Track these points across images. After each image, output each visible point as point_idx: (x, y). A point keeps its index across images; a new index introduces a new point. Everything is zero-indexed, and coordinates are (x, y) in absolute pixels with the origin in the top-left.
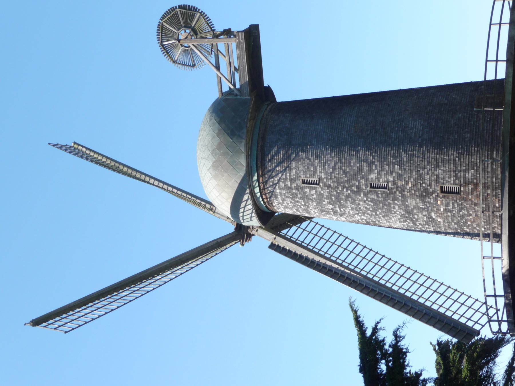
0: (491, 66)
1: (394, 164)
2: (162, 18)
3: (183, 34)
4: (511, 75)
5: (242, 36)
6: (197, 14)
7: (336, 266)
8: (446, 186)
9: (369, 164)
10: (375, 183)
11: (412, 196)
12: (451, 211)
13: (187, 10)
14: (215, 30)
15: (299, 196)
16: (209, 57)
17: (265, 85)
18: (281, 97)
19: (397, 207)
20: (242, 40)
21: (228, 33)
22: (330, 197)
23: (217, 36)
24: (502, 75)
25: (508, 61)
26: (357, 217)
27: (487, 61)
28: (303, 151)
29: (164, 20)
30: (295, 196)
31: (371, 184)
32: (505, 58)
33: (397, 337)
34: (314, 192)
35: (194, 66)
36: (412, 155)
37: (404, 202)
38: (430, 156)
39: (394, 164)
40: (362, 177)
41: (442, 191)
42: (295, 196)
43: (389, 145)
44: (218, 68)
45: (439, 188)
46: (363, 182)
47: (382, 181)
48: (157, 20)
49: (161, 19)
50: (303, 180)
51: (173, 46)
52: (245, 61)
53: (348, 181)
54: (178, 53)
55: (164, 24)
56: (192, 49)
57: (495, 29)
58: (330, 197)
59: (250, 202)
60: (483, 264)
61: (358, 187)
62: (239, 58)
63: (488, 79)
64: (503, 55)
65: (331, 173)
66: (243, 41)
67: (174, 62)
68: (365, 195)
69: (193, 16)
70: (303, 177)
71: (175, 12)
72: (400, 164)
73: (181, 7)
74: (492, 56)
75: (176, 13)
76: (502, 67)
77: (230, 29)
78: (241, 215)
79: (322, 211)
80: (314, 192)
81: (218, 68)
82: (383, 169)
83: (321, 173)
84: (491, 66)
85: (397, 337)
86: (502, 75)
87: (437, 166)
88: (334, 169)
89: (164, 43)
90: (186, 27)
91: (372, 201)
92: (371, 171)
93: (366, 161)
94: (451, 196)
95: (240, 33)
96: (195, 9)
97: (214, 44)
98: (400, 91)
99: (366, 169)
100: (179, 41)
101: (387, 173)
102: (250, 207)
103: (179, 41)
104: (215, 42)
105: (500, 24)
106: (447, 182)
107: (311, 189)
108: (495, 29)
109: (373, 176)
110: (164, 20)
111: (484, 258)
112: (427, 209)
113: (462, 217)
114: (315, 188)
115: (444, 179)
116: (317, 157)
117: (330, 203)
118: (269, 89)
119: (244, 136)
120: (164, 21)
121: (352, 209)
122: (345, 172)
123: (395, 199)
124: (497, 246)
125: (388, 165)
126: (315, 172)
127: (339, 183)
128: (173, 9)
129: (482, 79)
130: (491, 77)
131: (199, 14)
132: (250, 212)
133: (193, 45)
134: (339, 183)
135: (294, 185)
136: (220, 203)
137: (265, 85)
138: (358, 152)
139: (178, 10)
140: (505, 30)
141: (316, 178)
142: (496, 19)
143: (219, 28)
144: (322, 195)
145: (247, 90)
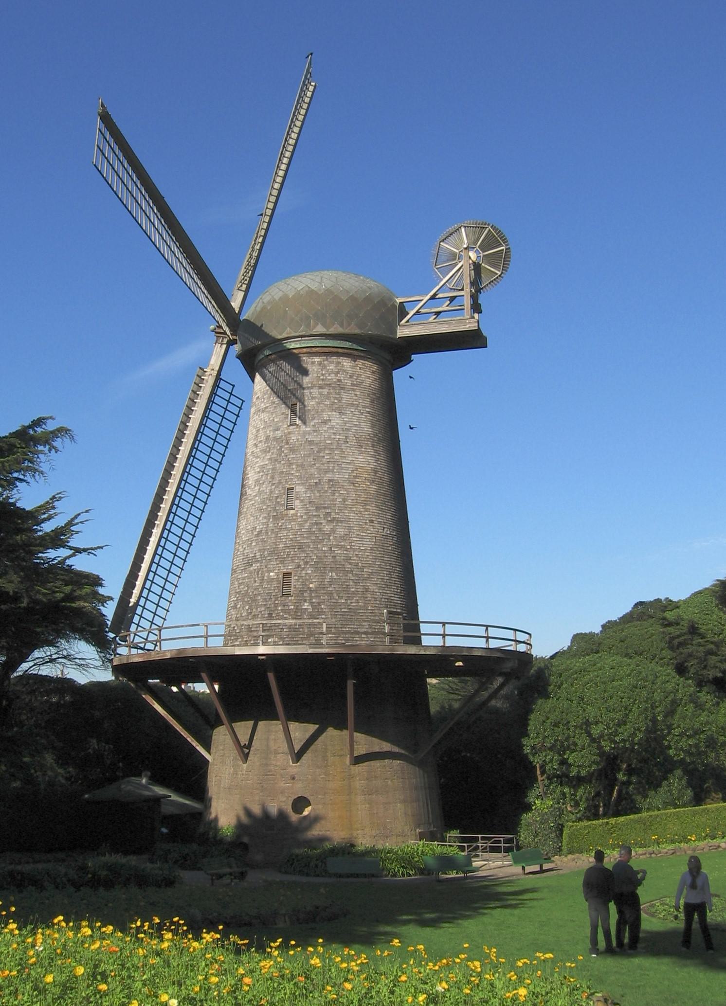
0: (439, 629)
6: (499, 271)
13: (504, 258)
14: (481, 293)
17: (413, 357)
18: (399, 376)
19: (265, 521)
20: (469, 327)
21: (476, 308)
29: (492, 230)
31: (293, 488)
33: (77, 532)
41: (287, 575)
49: (492, 226)
50: (296, 404)
55: (488, 229)
56: (456, 264)
57: (481, 631)
60: (198, 625)
64: (450, 642)
71: (501, 244)
75: (501, 245)
84: (439, 629)
85: (77, 532)
86: (426, 641)
89: (463, 229)
95: (477, 324)
96: (505, 269)
108: (481, 631)
110: (492, 230)
111: (207, 626)
120: (490, 230)
129: (421, 620)
130: (424, 629)
131: (499, 273)
133: (462, 266)
137: (413, 357)
140: (481, 643)
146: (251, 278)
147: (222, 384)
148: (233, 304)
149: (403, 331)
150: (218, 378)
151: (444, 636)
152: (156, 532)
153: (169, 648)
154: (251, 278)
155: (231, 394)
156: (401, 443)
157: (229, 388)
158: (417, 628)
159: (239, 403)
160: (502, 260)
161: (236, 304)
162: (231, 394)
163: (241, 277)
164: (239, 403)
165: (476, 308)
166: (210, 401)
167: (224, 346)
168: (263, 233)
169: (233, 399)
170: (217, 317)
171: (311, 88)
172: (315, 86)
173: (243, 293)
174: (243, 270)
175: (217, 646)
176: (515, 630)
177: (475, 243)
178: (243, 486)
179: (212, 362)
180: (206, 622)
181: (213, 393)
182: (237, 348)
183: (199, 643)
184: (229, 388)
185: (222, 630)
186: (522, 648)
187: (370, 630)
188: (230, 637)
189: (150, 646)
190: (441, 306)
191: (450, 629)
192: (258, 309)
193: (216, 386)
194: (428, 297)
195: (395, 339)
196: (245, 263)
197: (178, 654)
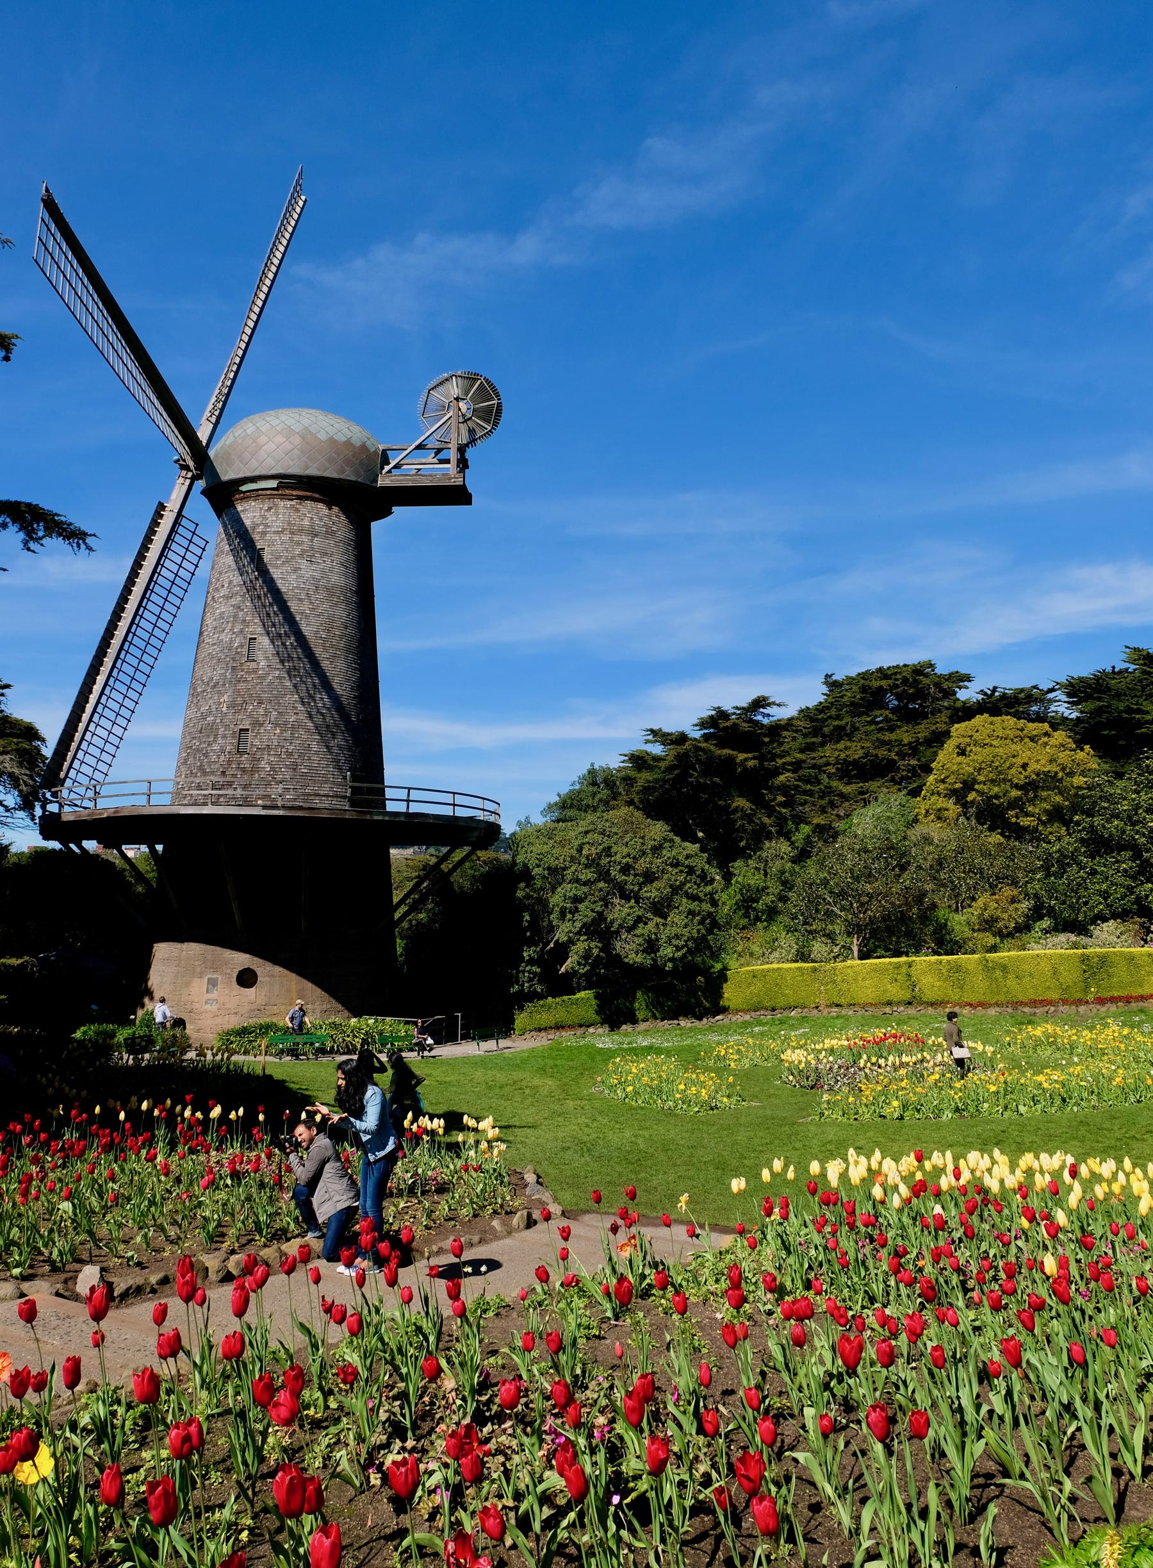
0: (403, 794)
5: (459, 482)
17: (394, 509)
21: (463, 464)
24: (391, 807)
26: (209, 621)
27: (409, 789)
47: (259, 655)
57: (449, 798)
64: (415, 808)
69: (488, 422)
73: (499, 405)
74: (414, 795)
75: (492, 399)
76: (401, 807)
77: (467, 467)
86: (391, 807)
94: (235, 741)
96: (496, 424)
97: (450, 446)
98: (378, 682)
105: (454, 805)
108: (449, 798)
109: (265, 641)
113: (206, 755)
124: (167, 799)
130: (389, 793)
136: (236, 434)
137: (394, 509)
140: (447, 811)
142: (459, 800)
143: (469, 454)
146: (222, 410)
147: (184, 522)
148: (199, 434)
149: (382, 482)
150: (180, 514)
151: (408, 801)
152: (101, 679)
153: (109, 804)
154: (222, 410)
155: (194, 533)
157: (192, 527)
158: (382, 792)
160: (493, 415)
161: (203, 434)
162: (194, 533)
163: (210, 407)
165: (463, 464)
166: (169, 538)
167: (188, 482)
168: (237, 360)
169: (196, 539)
170: (180, 449)
171: (301, 203)
172: (305, 202)
174: (214, 399)
175: (163, 804)
178: (201, 634)
179: (174, 496)
180: (150, 778)
181: (173, 530)
182: (201, 484)
183: (141, 801)
184: (192, 527)
185: (170, 787)
186: (492, 819)
187: (331, 794)
188: (178, 794)
189: (86, 803)
190: (426, 457)
192: (228, 443)
193: (176, 522)
194: (413, 447)
195: (376, 488)
196: (217, 391)
197: (116, 812)
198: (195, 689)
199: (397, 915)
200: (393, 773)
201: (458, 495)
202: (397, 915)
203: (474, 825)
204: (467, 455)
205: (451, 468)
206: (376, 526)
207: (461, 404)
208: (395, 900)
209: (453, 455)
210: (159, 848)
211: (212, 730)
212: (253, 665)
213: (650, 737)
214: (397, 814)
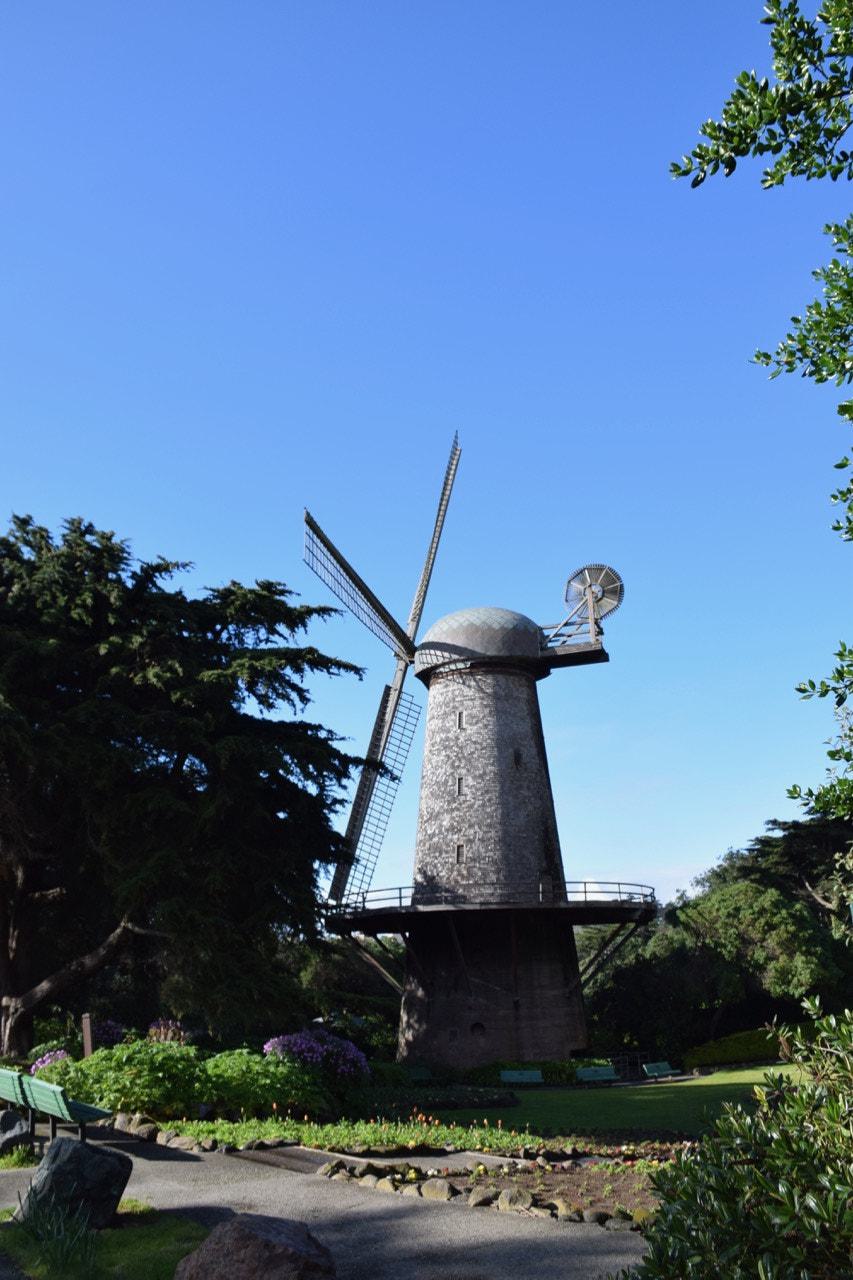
1: (483, 800)
2: (610, 569)
3: (597, 589)
4: (571, 906)
5: (598, 647)
7: (381, 749)
8: (465, 850)
9: (481, 776)
10: (464, 783)
11: (453, 818)
12: (440, 855)
15: (447, 710)
16: (576, 616)
17: (552, 670)
18: (540, 684)
21: (600, 632)
22: (447, 739)
23: (597, 623)
24: (571, 897)
25: (586, 902)
27: (585, 883)
28: (490, 712)
30: (447, 705)
32: (588, 899)
34: (452, 723)
35: (567, 601)
36: (492, 817)
37: (447, 811)
38: (493, 834)
39: (483, 800)
40: (468, 771)
42: (447, 705)
43: (501, 794)
44: (566, 624)
45: (462, 843)
46: (464, 771)
47: (465, 790)
48: (608, 563)
51: (583, 582)
52: (574, 650)
53: (464, 757)
54: (577, 586)
57: (615, 888)
58: (447, 739)
59: (441, 660)
61: (458, 767)
62: (577, 645)
63: (567, 885)
64: (591, 897)
65: (470, 740)
66: (593, 648)
67: (569, 582)
68: (452, 774)
70: (465, 713)
72: (483, 805)
73: (622, 586)
75: (615, 582)
76: (580, 898)
78: (427, 651)
79: (433, 733)
80: (452, 723)
81: (566, 624)
82: (477, 790)
83: (471, 730)
86: (571, 897)
87: (482, 840)
88: (475, 743)
90: (604, 592)
91: (446, 781)
92: (474, 778)
93: (485, 773)
94: (455, 855)
99: (477, 773)
100: (590, 586)
101: (473, 794)
102: (435, 661)
103: (590, 586)
104: (591, 621)
106: (468, 851)
107: (454, 721)
108: (615, 888)
109: (470, 781)
112: (440, 832)
114: (455, 724)
115: (471, 848)
116: (486, 726)
117: (441, 740)
118: (548, 674)
119: (501, 654)
121: (438, 762)
122: (473, 753)
123: (449, 803)
125: (482, 794)
126: (471, 724)
127: (461, 748)
128: (619, 578)
129: (567, 879)
130: (569, 887)
132: (430, 661)
134: (461, 748)
135: (457, 704)
137: (552, 670)
138: (492, 765)
139: (619, 584)
141: (464, 726)
143: (603, 624)
144: (449, 732)
145: (546, 653)
147: (403, 696)
156: (545, 740)
157: (410, 699)
159: (418, 709)
160: (618, 592)
164: (418, 709)
173: (415, 623)
176: (642, 886)
177: (597, 581)
184: (410, 699)
186: (649, 899)
191: (590, 887)
198: (422, 818)
199: (583, 978)
200: (571, 868)
201: (598, 656)
202: (583, 978)
203: (633, 906)
204: (602, 626)
205: (591, 638)
206: (540, 684)
207: (593, 588)
208: (581, 969)
209: (591, 627)
210: (407, 934)
211: (437, 849)
212: (462, 798)
213: (770, 826)
214: (578, 903)
